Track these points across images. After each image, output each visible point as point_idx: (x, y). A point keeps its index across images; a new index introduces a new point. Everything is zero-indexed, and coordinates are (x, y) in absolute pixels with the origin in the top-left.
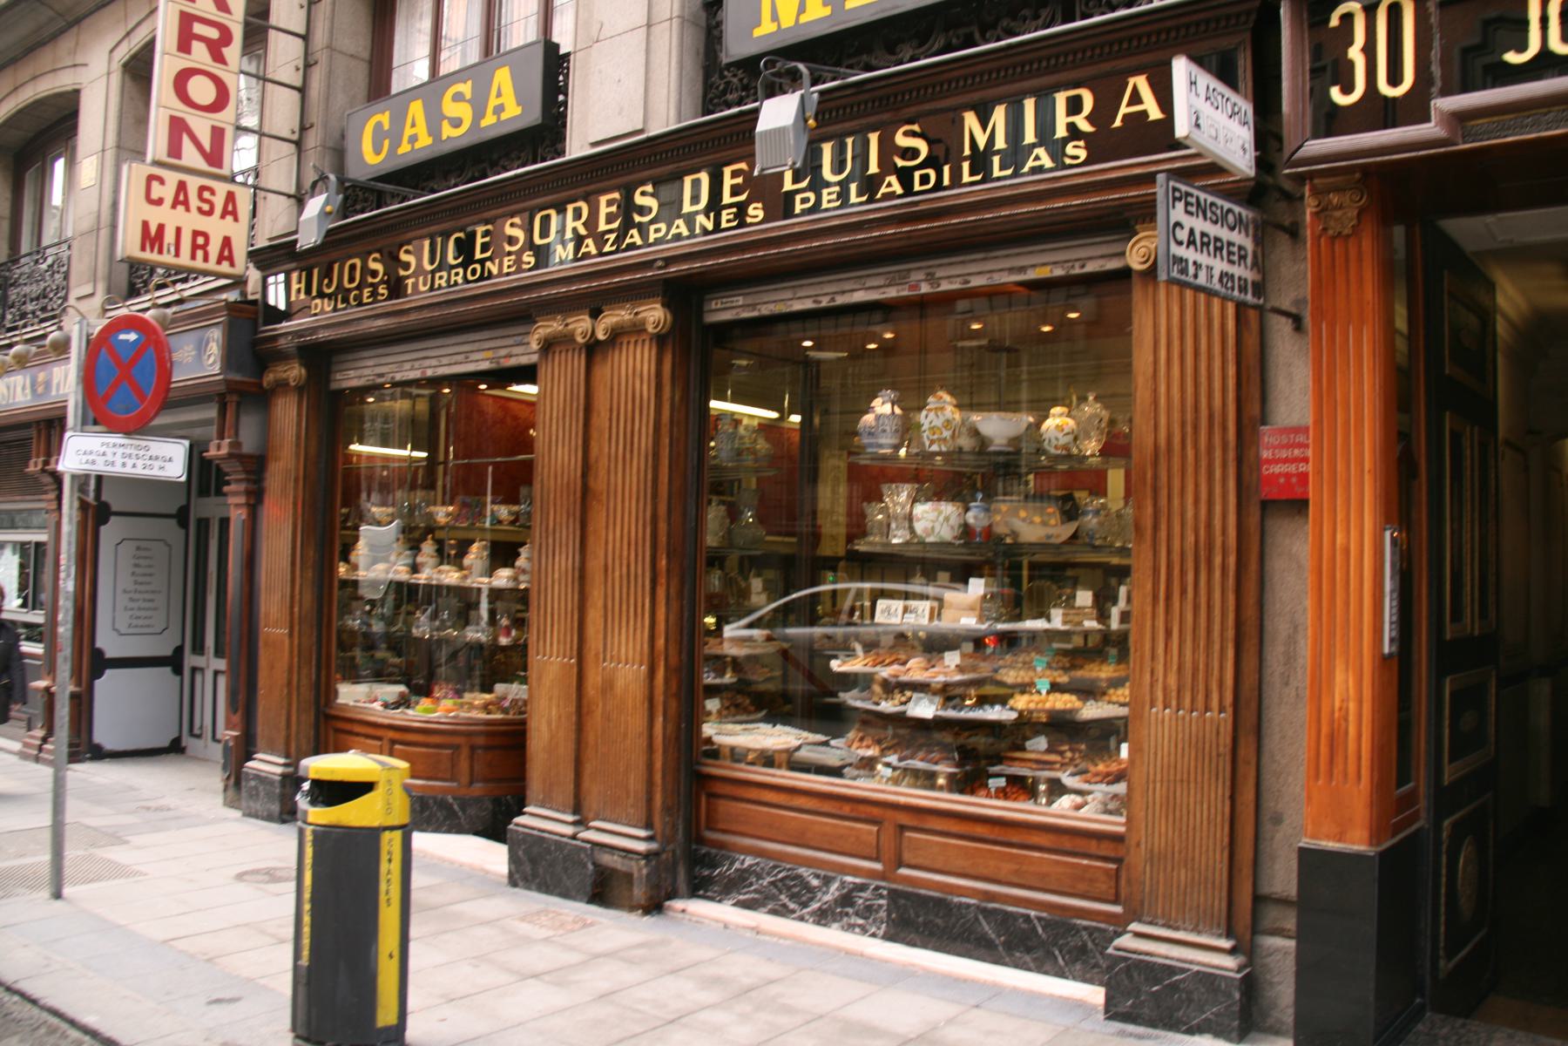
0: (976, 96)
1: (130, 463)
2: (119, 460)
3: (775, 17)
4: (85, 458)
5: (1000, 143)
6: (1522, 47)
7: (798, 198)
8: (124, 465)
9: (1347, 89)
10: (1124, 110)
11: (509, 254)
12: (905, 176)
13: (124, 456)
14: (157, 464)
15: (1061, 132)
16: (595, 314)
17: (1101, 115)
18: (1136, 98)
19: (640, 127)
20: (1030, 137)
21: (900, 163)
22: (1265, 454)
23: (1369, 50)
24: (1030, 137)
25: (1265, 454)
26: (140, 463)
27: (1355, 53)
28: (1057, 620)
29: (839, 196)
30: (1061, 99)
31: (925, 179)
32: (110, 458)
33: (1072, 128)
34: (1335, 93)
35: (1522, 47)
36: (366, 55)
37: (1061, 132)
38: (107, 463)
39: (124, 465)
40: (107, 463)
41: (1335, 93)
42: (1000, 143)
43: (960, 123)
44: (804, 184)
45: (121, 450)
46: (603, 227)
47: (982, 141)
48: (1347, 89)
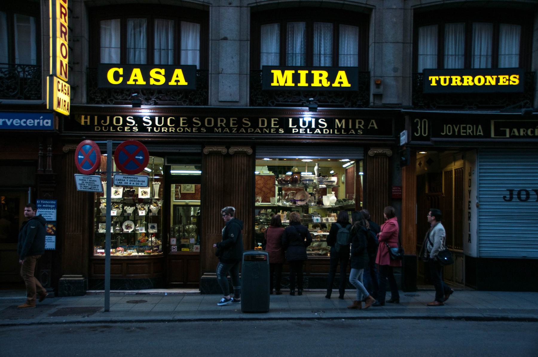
0: (339, 117)
1: (132, 183)
2: (129, 182)
3: (278, 82)
4: (119, 182)
5: (344, 127)
6: (443, 132)
7: (293, 130)
8: (130, 183)
9: (417, 133)
10: (370, 126)
11: (195, 127)
12: (321, 130)
13: (130, 181)
14: (140, 183)
15: (357, 127)
16: (228, 148)
17: (366, 125)
18: (372, 124)
19: (238, 100)
20: (350, 127)
21: (320, 127)
22: (393, 191)
23: (421, 128)
24: (350, 127)
25: (393, 191)
26: (135, 183)
27: (418, 127)
28: (44, 290)
29: (305, 131)
30: (357, 121)
31: (326, 131)
32: (126, 181)
33: (359, 127)
34: (415, 134)
35: (443, 132)
36: (119, 46)
37: (357, 127)
38: (125, 183)
39: (130, 183)
40: (125, 183)
41: (415, 134)
42: (344, 127)
43: (335, 121)
44: (295, 127)
45: (129, 179)
46: (231, 126)
47: (340, 126)
48: (417, 133)
